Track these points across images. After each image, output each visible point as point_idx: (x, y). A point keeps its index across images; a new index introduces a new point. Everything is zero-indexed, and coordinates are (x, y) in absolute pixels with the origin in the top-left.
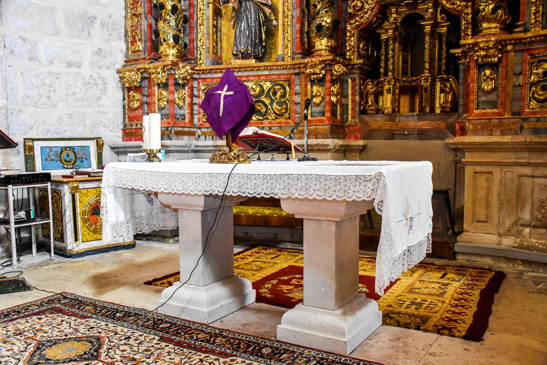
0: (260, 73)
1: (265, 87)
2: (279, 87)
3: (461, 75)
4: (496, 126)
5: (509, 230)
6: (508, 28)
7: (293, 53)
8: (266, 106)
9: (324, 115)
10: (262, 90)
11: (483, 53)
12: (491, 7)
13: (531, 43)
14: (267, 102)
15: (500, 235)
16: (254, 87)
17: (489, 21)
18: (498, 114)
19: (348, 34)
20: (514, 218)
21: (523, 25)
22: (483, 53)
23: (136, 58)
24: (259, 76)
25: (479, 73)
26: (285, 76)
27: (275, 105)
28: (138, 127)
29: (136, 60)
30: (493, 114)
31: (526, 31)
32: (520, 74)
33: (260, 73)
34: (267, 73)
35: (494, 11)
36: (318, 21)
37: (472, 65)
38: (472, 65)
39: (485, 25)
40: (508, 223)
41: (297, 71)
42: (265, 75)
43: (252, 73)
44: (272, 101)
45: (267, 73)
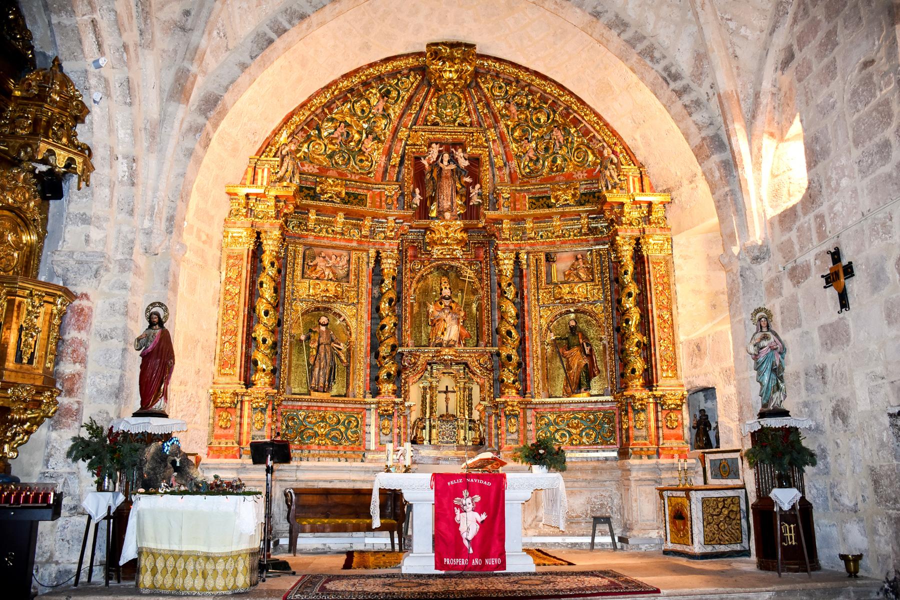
0: (337, 405)
1: (340, 417)
2: (354, 419)
5: (530, 525)
6: (523, 393)
7: (365, 392)
8: (341, 433)
10: (339, 420)
11: (511, 408)
12: (512, 379)
14: (343, 430)
15: (525, 529)
19: (403, 381)
20: (533, 516)
21: (530, 393)
22: (511, 408)
24: (336, 408)
25: (507, 421)
26: (358, 410)
27: (349, 433)
28: (228, 446)
31: (532, 397)
33: (337, 405)
34: (343, 405)
35: (514, 382)
40: (529, 520)
42: (342, 408)
43: (329, 405)
44: (347, 429)
45: (343, 405)
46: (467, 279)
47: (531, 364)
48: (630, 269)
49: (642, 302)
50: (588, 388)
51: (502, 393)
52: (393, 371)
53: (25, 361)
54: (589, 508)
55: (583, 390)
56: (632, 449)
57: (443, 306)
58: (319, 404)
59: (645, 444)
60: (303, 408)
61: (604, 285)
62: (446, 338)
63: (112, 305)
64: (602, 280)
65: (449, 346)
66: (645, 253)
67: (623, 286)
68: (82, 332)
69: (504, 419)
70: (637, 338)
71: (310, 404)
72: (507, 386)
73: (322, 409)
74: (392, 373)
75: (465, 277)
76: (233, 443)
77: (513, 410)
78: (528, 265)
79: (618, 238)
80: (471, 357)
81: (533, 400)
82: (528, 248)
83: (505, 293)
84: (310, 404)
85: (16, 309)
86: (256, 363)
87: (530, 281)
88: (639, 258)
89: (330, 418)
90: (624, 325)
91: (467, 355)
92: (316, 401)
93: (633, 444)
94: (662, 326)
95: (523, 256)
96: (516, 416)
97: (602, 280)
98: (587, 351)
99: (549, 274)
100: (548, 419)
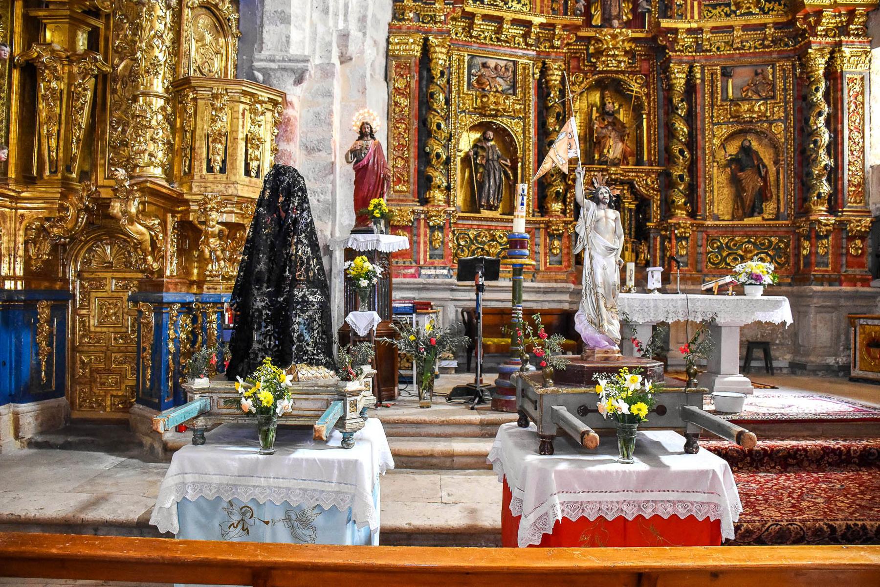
3: (652, 241)
4: (689, 279)
6: (692, 215)
7: (533, 211)
9: (561, 264)
12: (683, 200)
13: (708, 227)
16: (502, 235)
17: (682, 209)
18: (689, 271)
19: (568, 200)
22: (683, 230)
23: (401, 198)
25: (677, 243)
29: (402, 201)
30: (686, 270)
32: (701, 246)
35: (685, 203)
36: (554, 189)
37: (673, 237)
38: (673, 237)
39: (678, 212)
41: (537, 226)
46: (634, 94)
47: (702, 185)
48: (823, 85)
49: (834, 122)
50: (761, 212)
51: (672, 216)
52: (561, 189)
53: (253, 174)
54: (759, 333)
55: (756, 214)
56: (813, 275)
57: (606, 123)
58: (489, 223)
59: (827, 271)
60: (474, 227)
61: (786, 103)
62: (611, 156)
63: (317, 115)
64: (785, 98)
65: (616, 165)
66: (838, 67)
67: (813, 105)
68: (291, 143)
69: (674, 242)
70: (825, 160)
71: (480, 223)
72: (679, 207)
73: (474, 227)
74: (561, 191)
75: (632, 91)
76: (411, 263)
77: (685, 233)
78: (703, 80)
79: (810, 51)
80: (637, 176)
81: (704, 222)
82: (703, 62)
83: (677, 109)
84: (480, 223)
85: (241, 117)
86: (429, 179)
87: (703, 98)
88: (833, 75)
89: (500, 237)
90: (812, 146)
91: (634, 174)
92: (486, 219)
93: (815, 271)
94: (853, 149)
95: (697, 70)
96: (686, 238)
97: (785, 98)
98: (763, 174)
99: (725, 89)
100: (720, 242)
